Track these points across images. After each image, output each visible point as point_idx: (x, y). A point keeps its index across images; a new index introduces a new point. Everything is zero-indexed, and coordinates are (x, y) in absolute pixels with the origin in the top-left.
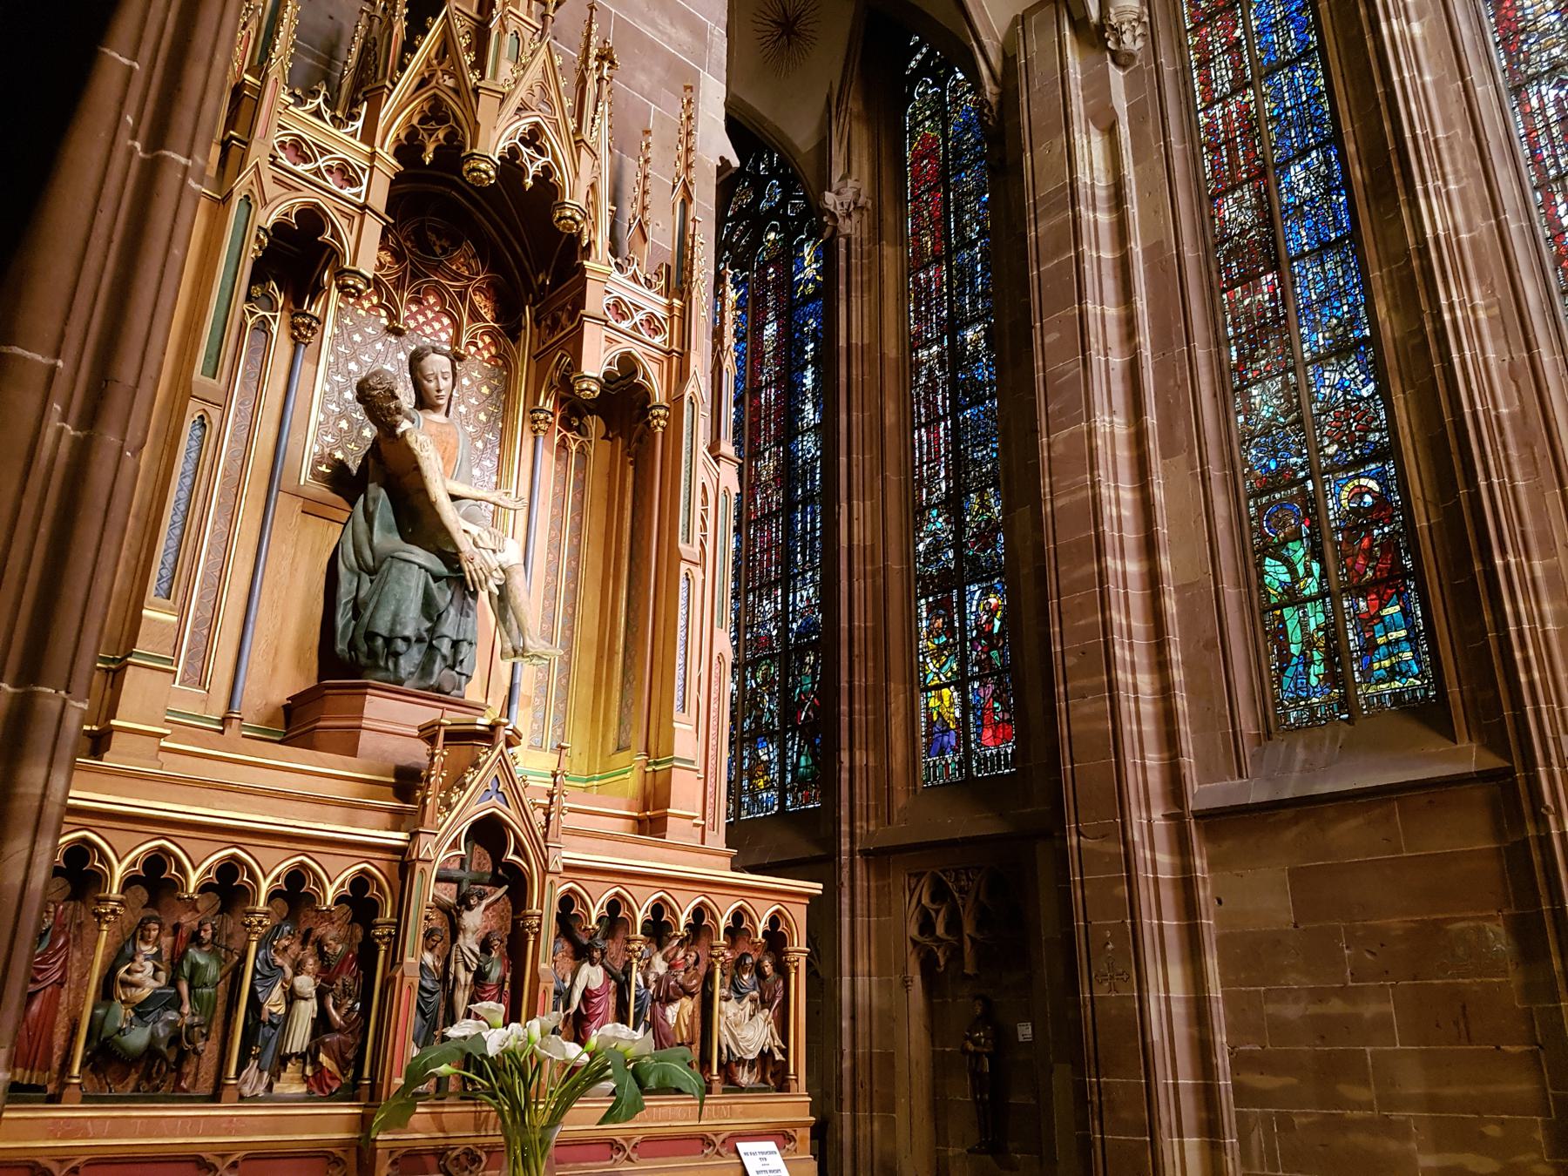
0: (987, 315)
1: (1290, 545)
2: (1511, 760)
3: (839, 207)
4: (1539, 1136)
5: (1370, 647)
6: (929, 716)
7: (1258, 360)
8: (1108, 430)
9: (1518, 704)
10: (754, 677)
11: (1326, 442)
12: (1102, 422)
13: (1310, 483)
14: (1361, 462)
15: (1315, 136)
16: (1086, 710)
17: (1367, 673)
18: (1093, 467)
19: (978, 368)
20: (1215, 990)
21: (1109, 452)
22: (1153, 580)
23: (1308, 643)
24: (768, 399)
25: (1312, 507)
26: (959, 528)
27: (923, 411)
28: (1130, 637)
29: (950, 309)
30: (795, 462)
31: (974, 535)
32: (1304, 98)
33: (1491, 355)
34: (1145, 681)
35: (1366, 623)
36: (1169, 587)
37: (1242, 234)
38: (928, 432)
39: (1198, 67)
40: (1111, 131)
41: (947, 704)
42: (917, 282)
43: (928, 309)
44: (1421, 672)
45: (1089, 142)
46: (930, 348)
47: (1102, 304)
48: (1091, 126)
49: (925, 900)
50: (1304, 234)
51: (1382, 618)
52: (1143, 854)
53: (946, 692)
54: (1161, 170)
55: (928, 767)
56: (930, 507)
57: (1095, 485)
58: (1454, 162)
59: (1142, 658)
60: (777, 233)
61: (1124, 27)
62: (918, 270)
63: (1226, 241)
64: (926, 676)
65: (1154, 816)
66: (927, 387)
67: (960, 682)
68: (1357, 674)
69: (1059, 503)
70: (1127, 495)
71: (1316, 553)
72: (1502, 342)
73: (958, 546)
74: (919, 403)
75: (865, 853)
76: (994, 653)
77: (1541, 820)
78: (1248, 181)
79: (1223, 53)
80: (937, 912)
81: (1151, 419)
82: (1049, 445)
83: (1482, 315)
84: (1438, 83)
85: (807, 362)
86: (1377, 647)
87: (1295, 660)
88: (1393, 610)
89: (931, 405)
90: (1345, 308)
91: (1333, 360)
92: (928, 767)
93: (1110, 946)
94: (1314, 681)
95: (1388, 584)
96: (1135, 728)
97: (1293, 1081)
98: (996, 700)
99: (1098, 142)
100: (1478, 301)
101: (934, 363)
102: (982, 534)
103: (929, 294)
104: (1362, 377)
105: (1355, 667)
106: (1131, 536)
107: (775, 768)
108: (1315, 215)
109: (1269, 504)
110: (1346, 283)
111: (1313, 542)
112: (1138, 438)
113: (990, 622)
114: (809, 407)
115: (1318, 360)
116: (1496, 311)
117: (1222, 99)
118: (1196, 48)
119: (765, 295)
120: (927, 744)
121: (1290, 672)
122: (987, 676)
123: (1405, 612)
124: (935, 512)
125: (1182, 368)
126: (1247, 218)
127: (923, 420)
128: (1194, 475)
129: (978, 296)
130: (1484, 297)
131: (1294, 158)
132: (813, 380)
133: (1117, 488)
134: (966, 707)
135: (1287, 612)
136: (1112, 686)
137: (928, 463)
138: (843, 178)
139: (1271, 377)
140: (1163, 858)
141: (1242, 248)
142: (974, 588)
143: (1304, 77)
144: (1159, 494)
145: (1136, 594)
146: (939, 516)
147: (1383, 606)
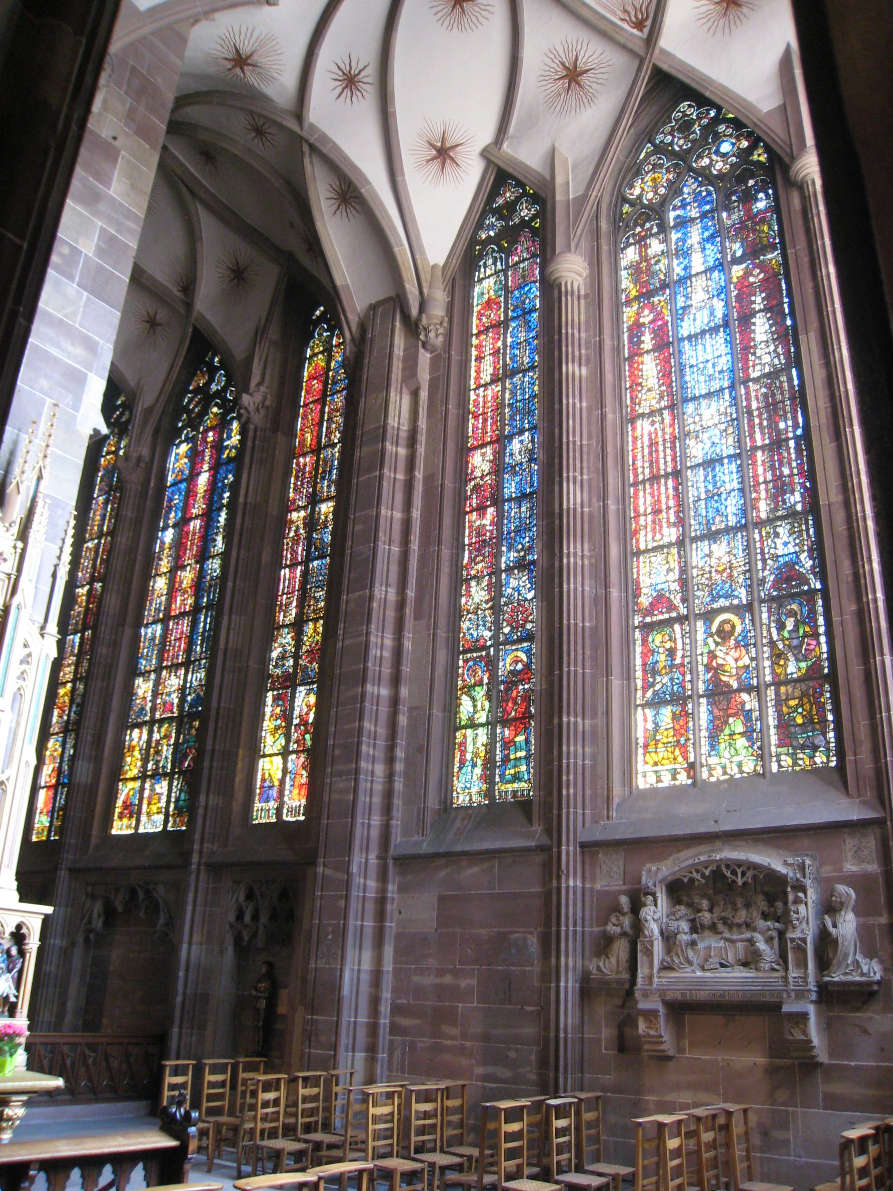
1: (477, 688)
2: (551, 840)
3: (252, 404)
4: (533, 1057)
5: (506, 760)
6: (263, 775)
7: (478, 563)
8: (383, 596)
9: (560, 808)
10: (159, 732)
11: (505, 624)
12: (379, 591)
13: (492, 649)
14: (520, 640)
15: (529, 422)
16: (341, 785)
17: (502, 776)
18: (369, 621)
20: (388, 966)
21: (382, 612)
22: (395, 701)
23: (476, 755)
24: (195, 527)
25: (491, 664)
26: (298, 643)
28: (375, 739)
30: (205, 577)
31: (307, 651)
32: (527, 396)
33: (587, 588)
34: (380, 769)
35: (508, 744)
36: (403, 708)
37: (482, 478)
39: (476, 360)
40: (415, 394)
42: (298, 464)
43: (302, 484)
44: (529, 779)
46: (299, 512)
47: (392, 510)
49: (242, 898)
50: (513, 485)
51: (515, 742)
52: (358, 880)
57: (368, 634)
58: (588, 460)
59: (380, 754)
60: (219, 409)
61: (432, 327)
62: (300, 456)
64: (265, 746)
65: (370, 857)
67: (285, 753)
68: (497, 776)
69: (347, 643)
70: (389, 642)
71: (488, 696)
72: (593, 581)
73: (296, 657)
74: (287, 550)
75: (209, 866)
77: (559, 877)
79: (490, 354)
80: (247, 907)
81: (411, 593)
82: (347, 602)
83: (586, 562)
84: (589, 408)
85: (223, 506)
86: (510, 760)
87: (467, 763)
88: (521, 738)
89: (294, 552)
90: (527, 539)
91: (516, 571)
93: (330, 937)
94: (475, 778)
95: (521, 722)
96: (368, 799)
97: (418, 1022)
99: (406, 401)
100: (586, 553)
101: (300, 523)
102: (312, 651)
103: (304, 474)
104: (529, 586)
105: (497, 771)
106: (387, 671)
107: (164, 799)
108: (521, 474)
110: (530, 523)
111: (488, 688)
112: (401, 605)
113: (307, 714)
114: (219, 539)
115: (509, 570)
116: (593, 561)
117: (485, 386)
119: (203, 451)
120: (260, 794)
121: (463, 771)
123: (527, 741)
124: (286, 630)
126: (486, 467)
127: (288, 563)
128: (429, 635)
130: (590, 550)
131: (516, 434)
132: (226, 519)
133: (382, 637)
134: (285, 771)
135: (469, 732)
136: (357, 771)
138: (259, 385)
140: (372, 884)
142: (301, 688)
143: (529, 383)
144: (407, 644)
145: (384, 710)
146: (288, 633)
147: (516, 735)
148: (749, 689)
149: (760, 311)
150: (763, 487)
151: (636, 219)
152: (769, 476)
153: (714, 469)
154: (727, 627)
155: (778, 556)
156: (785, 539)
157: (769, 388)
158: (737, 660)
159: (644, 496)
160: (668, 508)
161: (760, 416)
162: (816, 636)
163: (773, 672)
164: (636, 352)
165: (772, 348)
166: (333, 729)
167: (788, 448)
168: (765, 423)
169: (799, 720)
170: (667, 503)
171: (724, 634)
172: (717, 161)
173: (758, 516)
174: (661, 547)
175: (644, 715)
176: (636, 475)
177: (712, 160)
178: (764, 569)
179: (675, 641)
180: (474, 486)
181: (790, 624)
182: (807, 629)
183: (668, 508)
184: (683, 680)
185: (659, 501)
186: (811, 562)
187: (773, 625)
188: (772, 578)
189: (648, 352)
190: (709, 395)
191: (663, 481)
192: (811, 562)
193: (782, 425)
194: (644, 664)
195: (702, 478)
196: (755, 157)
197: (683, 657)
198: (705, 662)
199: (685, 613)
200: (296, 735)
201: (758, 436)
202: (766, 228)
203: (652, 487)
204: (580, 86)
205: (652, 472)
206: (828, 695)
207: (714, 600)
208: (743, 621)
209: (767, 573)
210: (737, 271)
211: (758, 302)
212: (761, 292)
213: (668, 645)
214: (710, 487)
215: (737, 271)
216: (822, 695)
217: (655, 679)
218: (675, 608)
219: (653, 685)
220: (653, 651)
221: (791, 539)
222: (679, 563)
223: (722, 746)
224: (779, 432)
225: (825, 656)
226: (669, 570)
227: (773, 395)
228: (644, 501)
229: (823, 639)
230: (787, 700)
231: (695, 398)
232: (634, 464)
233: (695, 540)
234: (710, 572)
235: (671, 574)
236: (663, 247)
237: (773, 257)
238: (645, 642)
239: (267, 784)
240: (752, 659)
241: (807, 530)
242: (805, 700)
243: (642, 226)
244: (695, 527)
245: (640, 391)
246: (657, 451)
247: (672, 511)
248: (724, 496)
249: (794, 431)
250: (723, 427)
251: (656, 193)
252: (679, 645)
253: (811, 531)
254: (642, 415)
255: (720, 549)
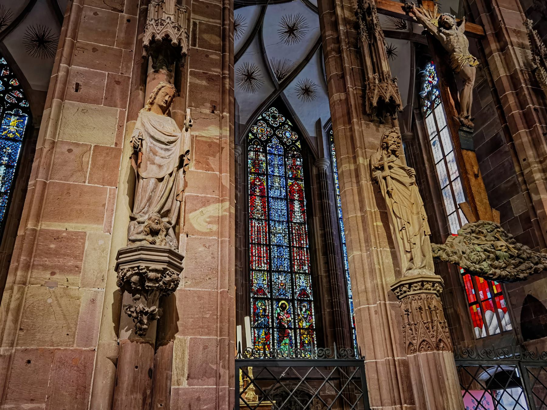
148: (291, 329)
149: (296, 200)
150: (296, 261)
151: (254, 142)
152: (298, 258)
153: (280, 248)
154: (284, 306)
155: (300, 286)
156: (303, 281)
157: (299, 228)
158: (287, 318)
159: (255, 249)
160: (264, 257)
161: (295, 236)
162: (311, 315)
163: (299, 324)
164: (253, 194)
165: (300, 214)
167: (304, 251)
168: (297, 239)
169: (307, 342)
170: (263, 255)
171: (283, 308)
172: (284, 138)
173: (294, 270)
174: (261, 271)
175: (254, 331)
176: (252, 240)
177: (282, 136)
178: (296, 289)
179: (266, 306)
181: (304, 309)
182: (309, 313)
183: (264, 257)
184: (269, 321)
185: (260, 253)
186: (310, 291)
187: (299, 309)
188: (299, 292)
189: (258, 196)
190: (279, 222)
191: (262, 246)
192: (310, 291)
193: (302, 242)
194: (254, 312)
195: (276, 250)
196: (297, 144)
197: (268, 313)
198: (276, 316)
199: (269, 297)
201: (295, 243)
202: (299, 172)
203: (258, 247)
204: (250, 82)
205: (258, 241)
206: (315, 335)
207: (280, 295)
208: (289, 305)
209: (297, 290)
210: (290, 182)
211: (296, 196)
212: (297, 194)
213: (263, 307)
214: (279, 254)
215: (290, 182)
216: (313, 335)
217: (258, 319)
218: (266, 295)
219: (258, 321)
220: (258, 308)
221: (305, 281)
222: (267, 278)
223: (282, 347)
224: (301, 244)
225: (314, 323)
226: (264, 280)
227: (300, 231)
228: (255, 251)
229: (313, 317)
230: (303, 335)
231: (275, 221)
232: (251, 236)
233: (273, 271)
234: (278, 285)
235: (265, 282)
236: (264, 159)
237: (302, 184)
238: (254, 304)
240: (292, 319)
241: (309, 280)
242: (308, 336)
243: (257, 146)
244: (274, 268)
245: (254, 209)
246: (260, 234)
247: (265, 258)
248: (283, 259)
249: (306, 246)
250: (283, 235)
251: (262, 136)
252: (267, 308)
253: (311, 281)
254: (255, 219)
255: (282, 278)
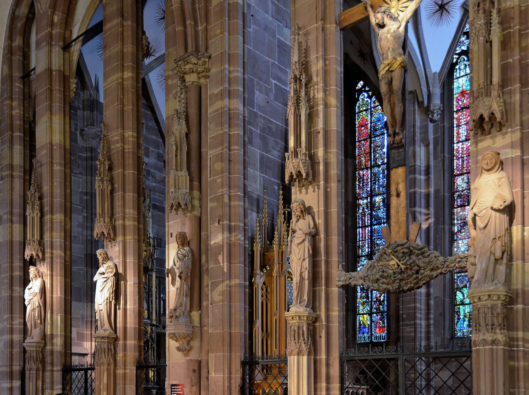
0: (383, 194)
6: (360, 323)
19: (379, 212)
27: (360, 222)
29: (371, 188)
38: (362, 230)
41: (366, 320)
45: (420, 150)
48: (421, 144)
53: (365, 316)
54: (441, 164)
55: (359, 337)
56: (362, 256)
63: (458, 192)
66: (362, 214)
76: (381, 306)
78: (466, 173)
92: (359, 337)
98: (380, 320)
109: (460, 276)
118: (456, 119)
120: (359, 331)
122: (378, 313)
125: (441, 232)
129: (381, 186)
134: (372, 321)
137: (362, 241)
139: (465, 239)
141: (462, 195)
145: (423, 298)
166: (401, 306)
180: (458, 195)
200: (375, 306)
239: (362, 326)
